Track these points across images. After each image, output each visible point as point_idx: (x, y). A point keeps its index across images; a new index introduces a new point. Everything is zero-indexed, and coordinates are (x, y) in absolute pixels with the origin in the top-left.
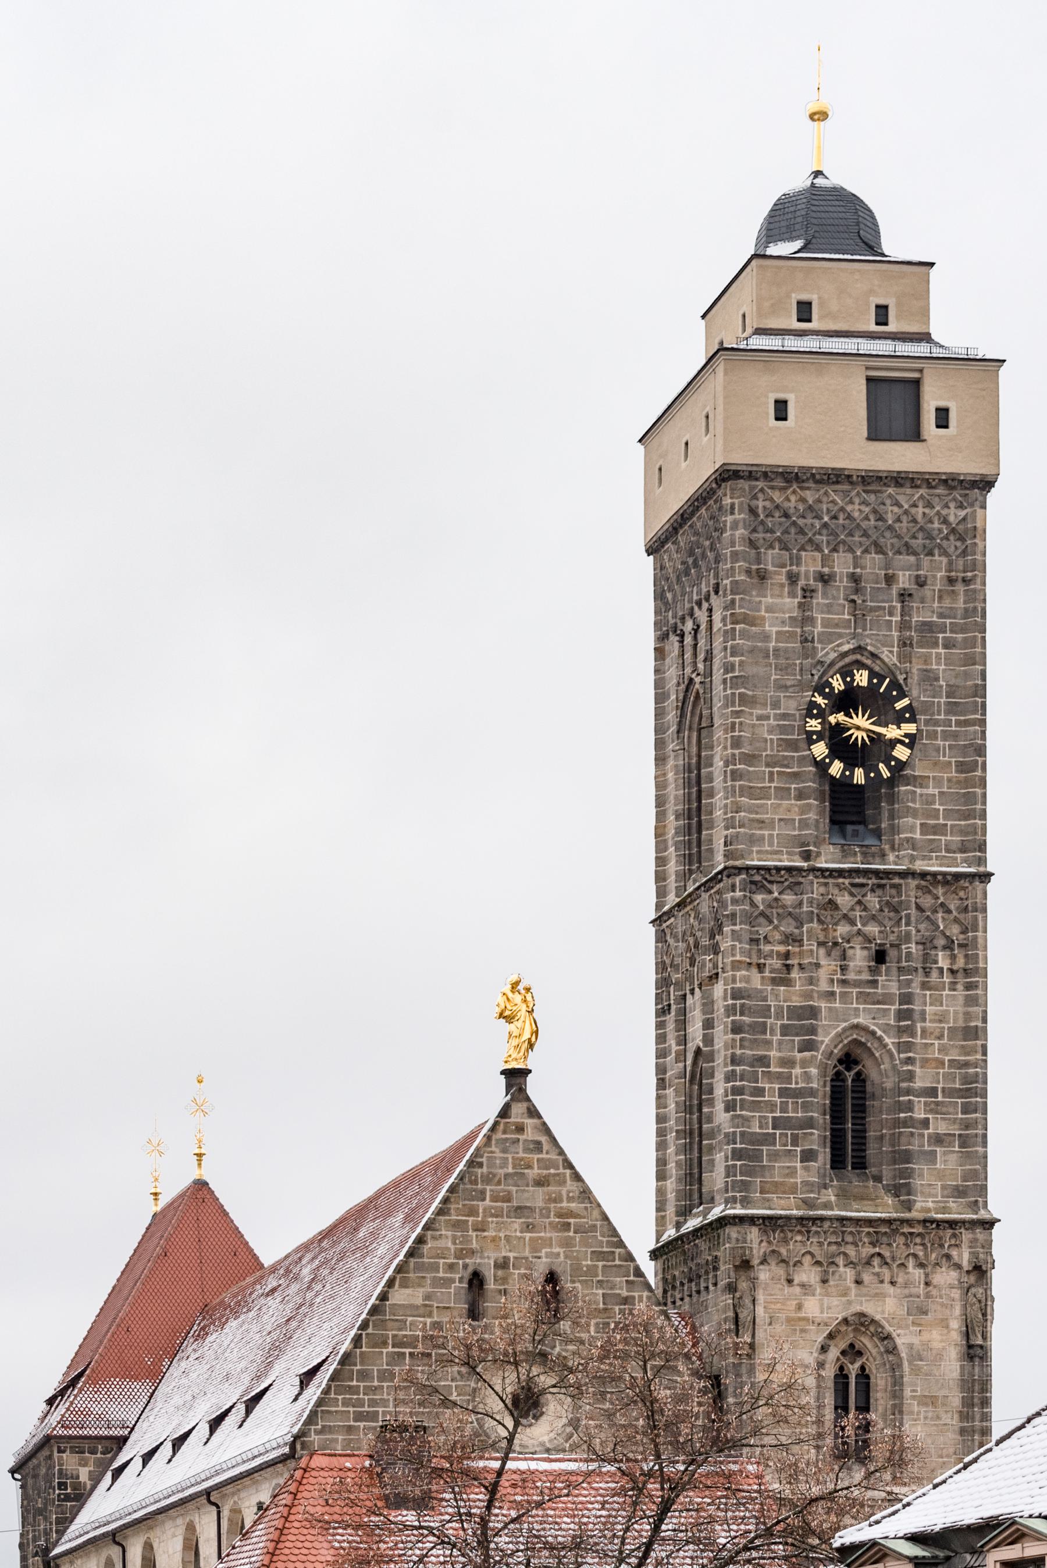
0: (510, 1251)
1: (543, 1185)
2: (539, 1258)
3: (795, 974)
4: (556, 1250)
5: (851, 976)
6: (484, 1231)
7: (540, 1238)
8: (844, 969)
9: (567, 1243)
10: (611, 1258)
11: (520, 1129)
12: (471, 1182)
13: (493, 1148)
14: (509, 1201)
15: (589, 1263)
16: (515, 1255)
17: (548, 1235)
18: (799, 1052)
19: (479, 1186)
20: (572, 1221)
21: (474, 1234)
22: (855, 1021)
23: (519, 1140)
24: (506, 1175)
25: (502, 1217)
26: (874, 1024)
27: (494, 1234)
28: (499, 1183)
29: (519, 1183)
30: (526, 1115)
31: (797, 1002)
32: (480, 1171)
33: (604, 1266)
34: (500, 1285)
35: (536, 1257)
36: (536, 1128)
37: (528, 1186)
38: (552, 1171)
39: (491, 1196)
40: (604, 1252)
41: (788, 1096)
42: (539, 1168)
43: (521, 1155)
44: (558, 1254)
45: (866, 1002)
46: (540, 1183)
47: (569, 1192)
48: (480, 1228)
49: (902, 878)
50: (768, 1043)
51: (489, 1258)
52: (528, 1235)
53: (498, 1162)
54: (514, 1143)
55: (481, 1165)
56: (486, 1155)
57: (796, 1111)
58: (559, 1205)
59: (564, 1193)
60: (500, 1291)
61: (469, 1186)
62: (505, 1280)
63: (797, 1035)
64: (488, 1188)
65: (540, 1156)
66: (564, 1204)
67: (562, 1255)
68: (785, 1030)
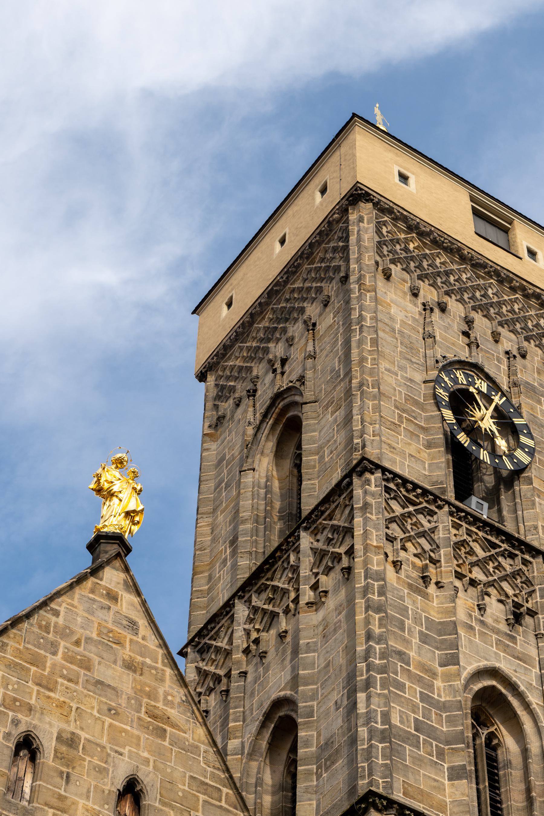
0: (82, 729)
1: (135, 671)
2: (121, 754)
3: (432, 589)
4: (146, 755)
5: (489, 620)
6: (50, 690)
7: (125, 731)
8: (481, 608)
9: (159, 753)
10: (216, 795)
11: (113, 597)
12: (40, 627)
13: (76, 602)
14: (88, 669)
15: (186, 788)
16: (87, 736)
17: (136, 732)
18: (441, 665)
19: (50, 636)
20: (169, 729)
21: (36, 688)
22: (497, 665)
23: (109, 608)
24: (88, 640)
25: (77, 683)
26: (516, 677)
27: (62, 699)
28: (77, 643)
29: (105, 655)
30: (121, 586)
31: (436, 617)
32: (54, 619)
33: (205, 801)
34: (62, 765)
35: (116, 752)
36: (132, 605)
37: (115, 662)
38: (148, 661)
39: (64, 653)
40: (207, 784)
41: (431, 704)
42: (130, 650)
43: (110, 626)
44: (147, 762)
45: (505, 651)
46: (130, 666)
47: (166, 694)
48: (46, 685)
49: (533, 557)
50: (407, 642)
51: (50, 724)
52: (108, 721)
53: (79, 619)
54: (102, 608)
55: (56, 614)
56: (64, 605)
57: (440, 723)
58: (153, 703)
59: (161, 691)
60: (62, 773)
61: (36, 629)
62: (69, 763)
63: (437, 649)
64: (62, 643)
65: (135, 638)
66: (160, 705)
67: (151, 763)
68: (424, 639)
